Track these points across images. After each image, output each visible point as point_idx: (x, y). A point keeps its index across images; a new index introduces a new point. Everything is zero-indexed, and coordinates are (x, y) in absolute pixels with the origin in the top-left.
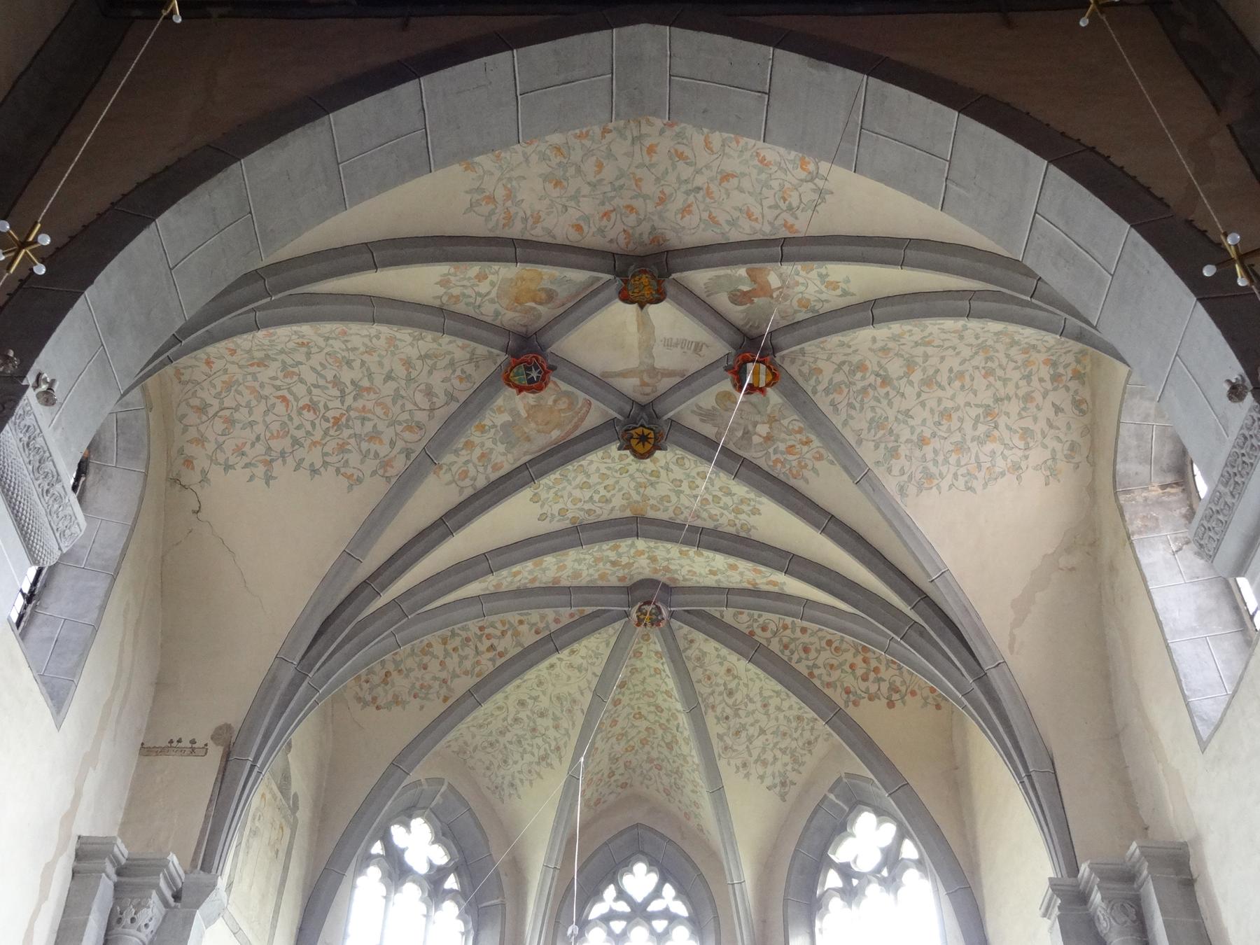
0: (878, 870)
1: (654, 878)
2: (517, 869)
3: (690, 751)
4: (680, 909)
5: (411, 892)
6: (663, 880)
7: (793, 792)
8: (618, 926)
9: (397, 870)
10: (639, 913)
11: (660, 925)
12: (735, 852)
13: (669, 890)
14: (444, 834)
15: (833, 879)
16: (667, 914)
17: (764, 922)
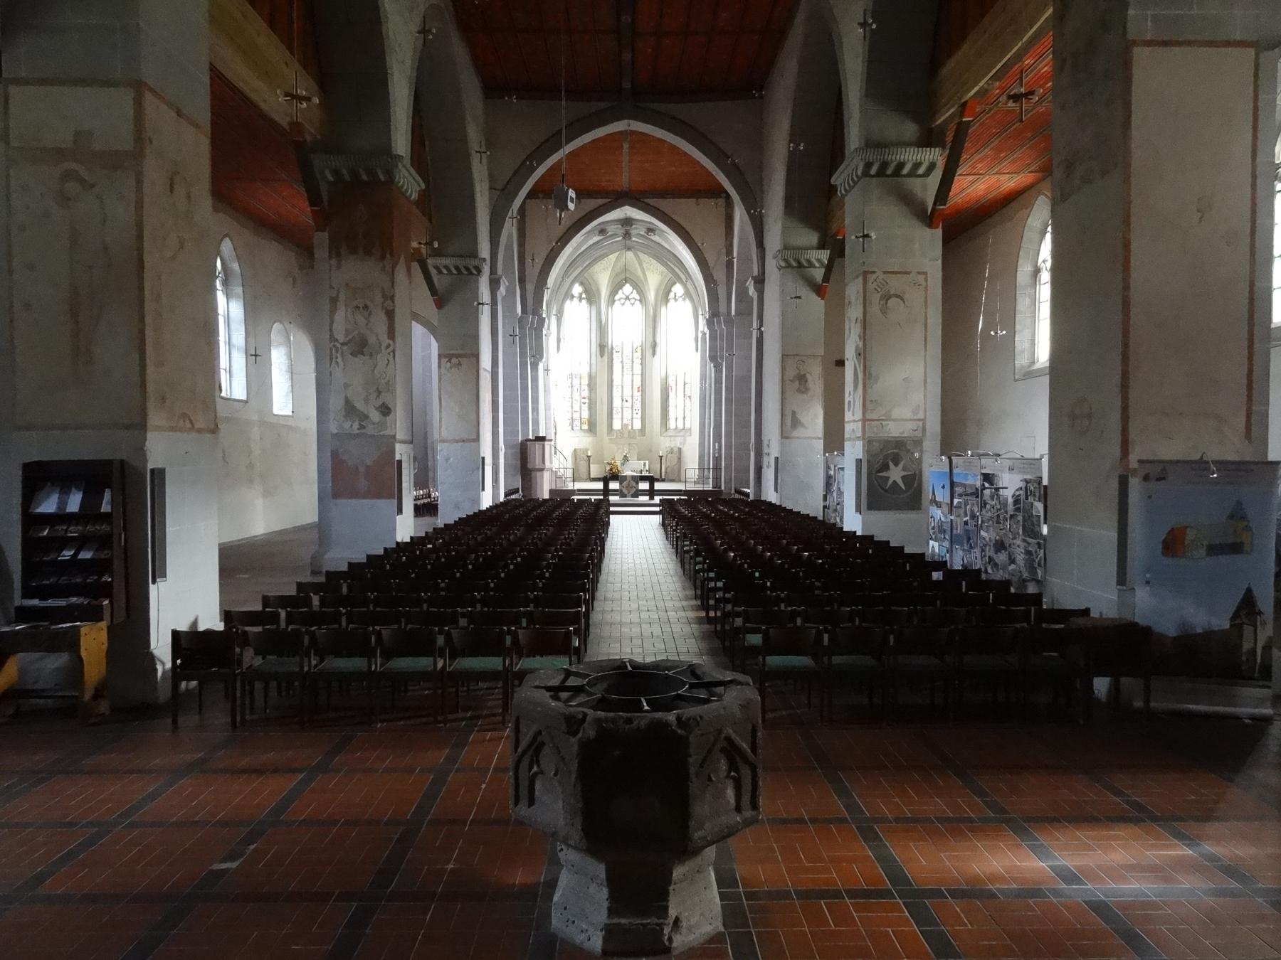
0: (681, 297)
1: (631, 288)
2: (598, 291)
3: (639, 270)
4: (638, 297)
5: (576, 300)
6: (633, 289)
7: (664, 274)
8: (622, 301)
9: (573, 297)
10: (627, 298)
11: (632, 301)
12: (649, 291)
13: (635, 292)
14: (582, 284)
15: (672, 295)
16: (634, 298)
17: (656, 305)
